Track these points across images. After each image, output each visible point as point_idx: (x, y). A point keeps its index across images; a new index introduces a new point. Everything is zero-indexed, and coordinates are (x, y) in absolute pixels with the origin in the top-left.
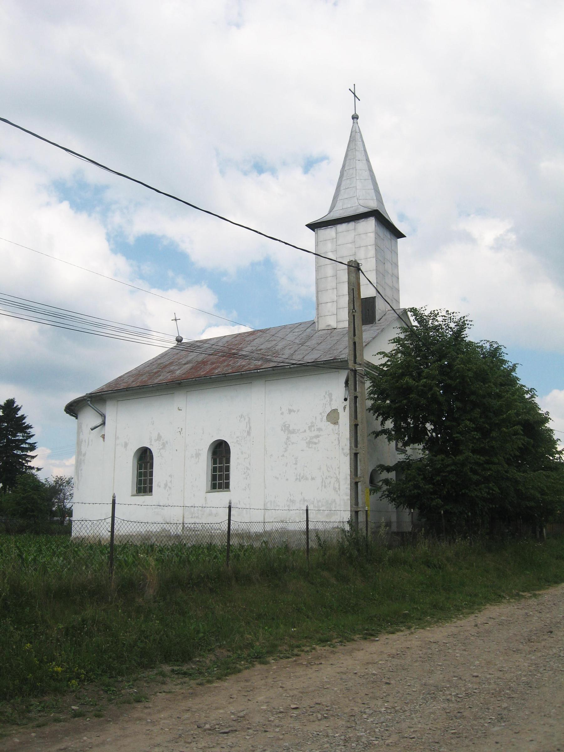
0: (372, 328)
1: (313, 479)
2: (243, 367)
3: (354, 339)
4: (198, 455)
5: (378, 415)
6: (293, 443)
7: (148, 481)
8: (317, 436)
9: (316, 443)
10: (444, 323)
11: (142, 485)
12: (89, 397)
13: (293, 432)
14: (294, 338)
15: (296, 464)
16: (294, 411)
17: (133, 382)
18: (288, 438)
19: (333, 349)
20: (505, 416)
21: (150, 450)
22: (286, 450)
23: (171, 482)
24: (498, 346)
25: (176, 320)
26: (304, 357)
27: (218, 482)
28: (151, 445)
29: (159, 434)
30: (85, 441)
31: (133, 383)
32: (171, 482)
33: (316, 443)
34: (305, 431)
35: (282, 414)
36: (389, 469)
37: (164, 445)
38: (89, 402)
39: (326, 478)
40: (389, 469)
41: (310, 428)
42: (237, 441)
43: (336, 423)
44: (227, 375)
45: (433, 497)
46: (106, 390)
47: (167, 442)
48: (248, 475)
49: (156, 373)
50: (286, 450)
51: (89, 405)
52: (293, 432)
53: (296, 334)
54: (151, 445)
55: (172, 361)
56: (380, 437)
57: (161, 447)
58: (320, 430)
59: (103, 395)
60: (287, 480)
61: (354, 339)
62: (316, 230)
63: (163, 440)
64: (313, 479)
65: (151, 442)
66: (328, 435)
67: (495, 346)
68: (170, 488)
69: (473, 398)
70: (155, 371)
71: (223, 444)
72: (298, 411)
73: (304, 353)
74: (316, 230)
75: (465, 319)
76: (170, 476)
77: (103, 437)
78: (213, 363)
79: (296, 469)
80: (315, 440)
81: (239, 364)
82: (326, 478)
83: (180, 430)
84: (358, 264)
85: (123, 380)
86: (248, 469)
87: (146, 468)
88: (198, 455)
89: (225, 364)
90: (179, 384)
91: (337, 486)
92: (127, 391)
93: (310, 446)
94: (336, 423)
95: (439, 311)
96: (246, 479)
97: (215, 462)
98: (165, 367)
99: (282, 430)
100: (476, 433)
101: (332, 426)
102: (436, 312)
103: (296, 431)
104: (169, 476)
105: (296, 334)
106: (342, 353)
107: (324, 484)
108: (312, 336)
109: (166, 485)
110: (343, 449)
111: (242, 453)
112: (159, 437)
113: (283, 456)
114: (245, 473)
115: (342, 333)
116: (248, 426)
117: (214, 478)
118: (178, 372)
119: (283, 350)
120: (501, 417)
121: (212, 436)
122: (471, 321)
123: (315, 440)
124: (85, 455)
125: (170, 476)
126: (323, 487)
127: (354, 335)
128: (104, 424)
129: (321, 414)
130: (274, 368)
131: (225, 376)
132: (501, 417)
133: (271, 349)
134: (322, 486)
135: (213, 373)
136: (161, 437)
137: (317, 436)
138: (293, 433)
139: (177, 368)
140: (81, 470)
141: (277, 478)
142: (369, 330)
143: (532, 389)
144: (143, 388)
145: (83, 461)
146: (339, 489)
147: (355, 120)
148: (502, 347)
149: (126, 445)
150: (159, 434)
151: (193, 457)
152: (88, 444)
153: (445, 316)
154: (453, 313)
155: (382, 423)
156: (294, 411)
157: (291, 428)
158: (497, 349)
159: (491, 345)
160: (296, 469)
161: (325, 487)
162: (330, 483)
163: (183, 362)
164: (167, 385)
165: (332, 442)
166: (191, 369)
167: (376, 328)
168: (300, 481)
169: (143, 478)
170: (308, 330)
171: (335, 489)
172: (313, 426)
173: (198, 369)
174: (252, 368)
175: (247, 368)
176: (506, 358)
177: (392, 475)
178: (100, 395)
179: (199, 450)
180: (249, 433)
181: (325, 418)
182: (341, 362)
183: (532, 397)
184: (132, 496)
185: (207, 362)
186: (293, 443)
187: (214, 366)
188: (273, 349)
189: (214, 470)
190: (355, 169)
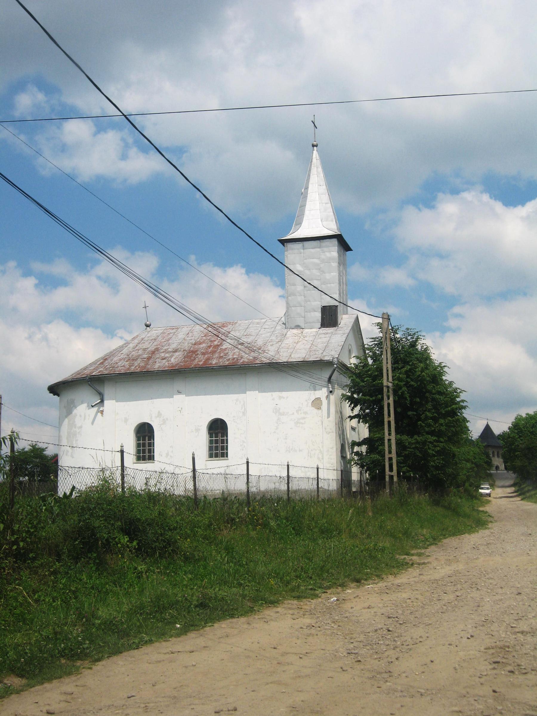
0: (338, 332)
1: (300, 451)
2: (237, 360)
3: (387, 366)
4: (197, 430)
5: (351, 404)
6: (283, 423)
7: (147, 451)
8: (304, 418)
9: (302, 423)
10: (404, 336)
11: (141, 454)
12: (90, 378)
13: (283, 414)
14: (269, 334)
15: (286, 439)
16: (284, 398)
17: (130, 366)
18: (278, 419)
19: (313, 349)
20: (449, 408)
21: (148, 423)
22: (277, 429)
23: (172, 451)
24: (427, 347)
25: (145, 307)
26: (291, 355)
27: (214, 452)
28: (151, 420)
29: (159, 412)
30: (81, 416)
31: (133, 367)
32: (172, 451)
33: (302, 423)
34: (293, 414)
35: (273, 399)
36: (359, 444)
37: (164, 422)
38: (89, 383)
39: (312, 450)
40: (359, 444)
41: (297, 411)
42: (234, 420)
43: (319, 408)
44: (228, 367)
45: (402, 465)
46: (106, 372)
47: (167, 419)
48: (244, 446)
49: (149, 358)
50: (277, 429)
51: (90, 385)
52: (283, 414)
53: (269, 330)
54: (151, 420)
55: (155, 347)
56: (353, 420)
57: (161, 423)
58: (306, 413)
59: (105, 377)
60: (278, 451)
61: (387, 366)
62: (285, 244)
63: (163, 417)
64: (300, 451)
65: (151, 418)
66: (313, 417)
67: (425, 347)
68: (171, 456)
69: (427, 395)
70: (145, 356)
71: (219, 422)
72: (287, 397)
73: (288, 351)
74: (285, 244)
75: (419, 333)
76: (171, 447)
77: (102, 412)
78: (203, 354)
79: (286, 443)
80: (301, 421)
81: (231, 357)
82: (312, 450)
83: (180, 409)
84: (389, 315)
85: (117, 363)
86: (244, 442)
87: (144, 440)
88: (197, 430)
89: (217, 355)
90: (180, 371)
91: (320, 456)
92: (131, 375)
93: (298, 425)
94: (319, 408)
95: (399, 326)
96: (243, 450)
97: (211, 435)
98: (153, 353)
99: (273, 412)
100: (431, 421)
101: (315, 411)
102: (397, 327)
103: (286, 413)
104: (171, 447)
105: (269, 330)
106: (324, 354)
107: (309, 455)
108: (286, 334)
109: (167, 454)
110: (325, 429)
111: (238, 429)
112: (159, 415)
113: (275, 432)
114: (241, 446)
115: (312, 334)
116: (243, 408)
117: (211, 449)
118: (173, 360)
119: (266, 346)
120: (447, 409)
121: (211, 415)
122: (424, 336)
123: (301, 421)
124: (81, 427)
125: (171, 447)
126: (309, 457)
127: (387, 363)
128: (102, 401)
129: (306, 401)
130: (271, 364)
131: (226, 368)
132: (447, 409)
133: (253, 344)
134: (308, 456)
135: (211, 364)
136: (161, 414)
137: (304, 418)
138: (284, 415)
139: (167, 355)
140: (77, 440)
141: (270, 450)
142: (335, 334)
143: (451, 382)
144: (147, 373)
145: (79, 433)
146: (323, 459)
147: (315, 148)
148: (430, 348)
149: (126, 420)
150: (159, 412)
151: (193, 431)
152: (85, 419)
153: (405, 331)
154: (411, 329)
155: (352, 410)
156: (284, 398)
157: (281, 411)
158: (426, 349)
159: (422, 347)
160: (286, 443)
161: (311, 457)
162: (315, 454)
163: (169, 350)
164: (171, 371)
165: (316, 423)
166: (185, 357)
167: (341, 332)
168: (289, 452)
169: (141, 448)
170: (279, 327)
171: (318, 458)
172: (300, 410)
173: (192, 358)
174: (246, 362)
175: (242, 361)
176: (433, 357)
177: (364, 449)
178: (99, 377)
179: (198, 426)
180: (244, 413)
181: (310, 404)
182: (327, 362)
183: (460, 392)
184: (134, 463)
185: (196, 351)
186: (283, 423)
187: (206, 356)
188: (255, 344)
189: (211, 442)
190: (317, 193)
